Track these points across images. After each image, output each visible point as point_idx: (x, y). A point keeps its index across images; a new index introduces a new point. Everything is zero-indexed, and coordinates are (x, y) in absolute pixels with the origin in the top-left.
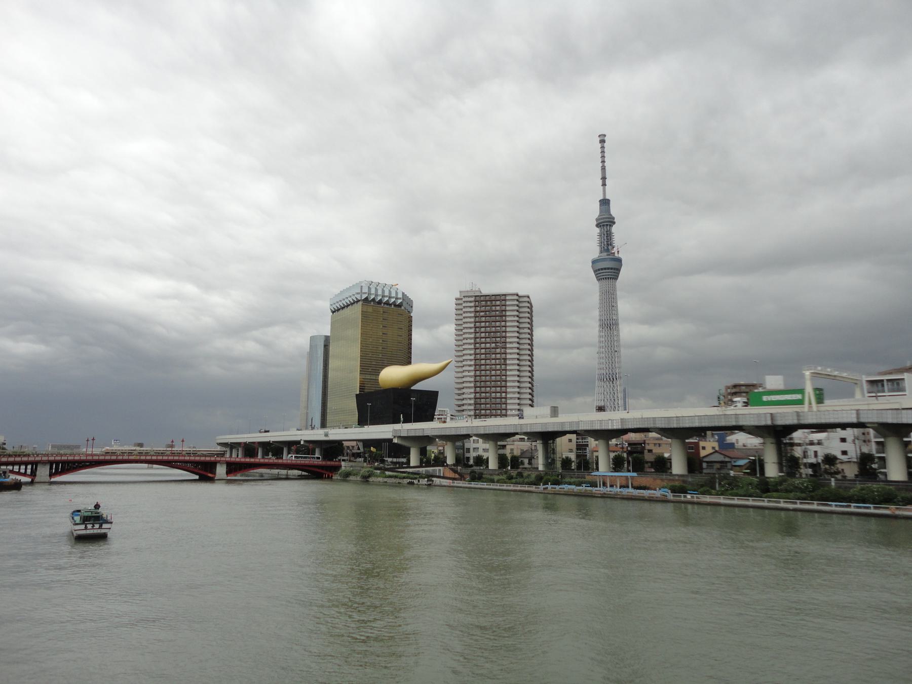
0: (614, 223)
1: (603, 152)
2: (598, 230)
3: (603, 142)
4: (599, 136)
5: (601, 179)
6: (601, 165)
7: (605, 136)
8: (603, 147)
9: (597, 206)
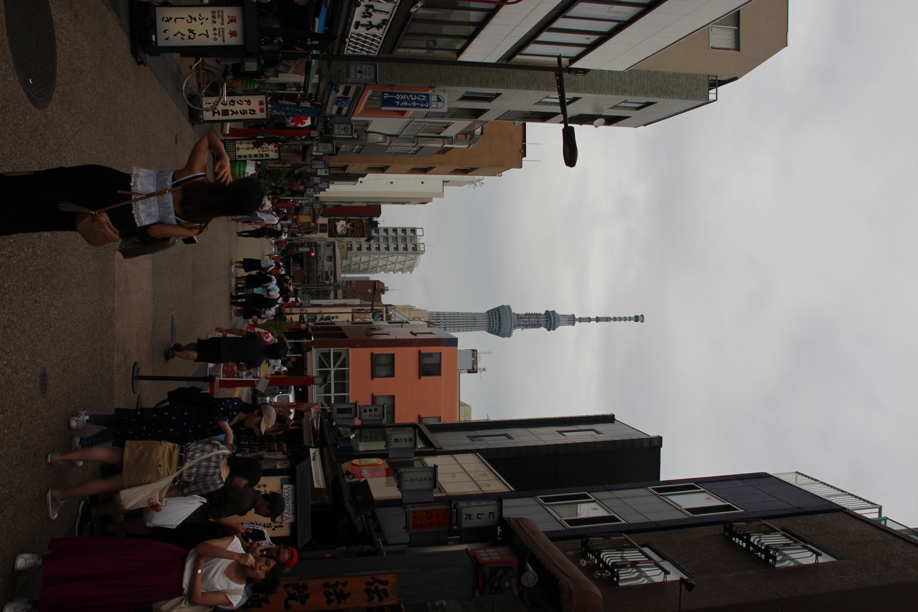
0: (549, 330)
2: (543, 312)
3: (637, 319)
4: (642, 315)
6: (612, 317)
7: (642, 322)
8: (630, 319)
9: (569, 312)
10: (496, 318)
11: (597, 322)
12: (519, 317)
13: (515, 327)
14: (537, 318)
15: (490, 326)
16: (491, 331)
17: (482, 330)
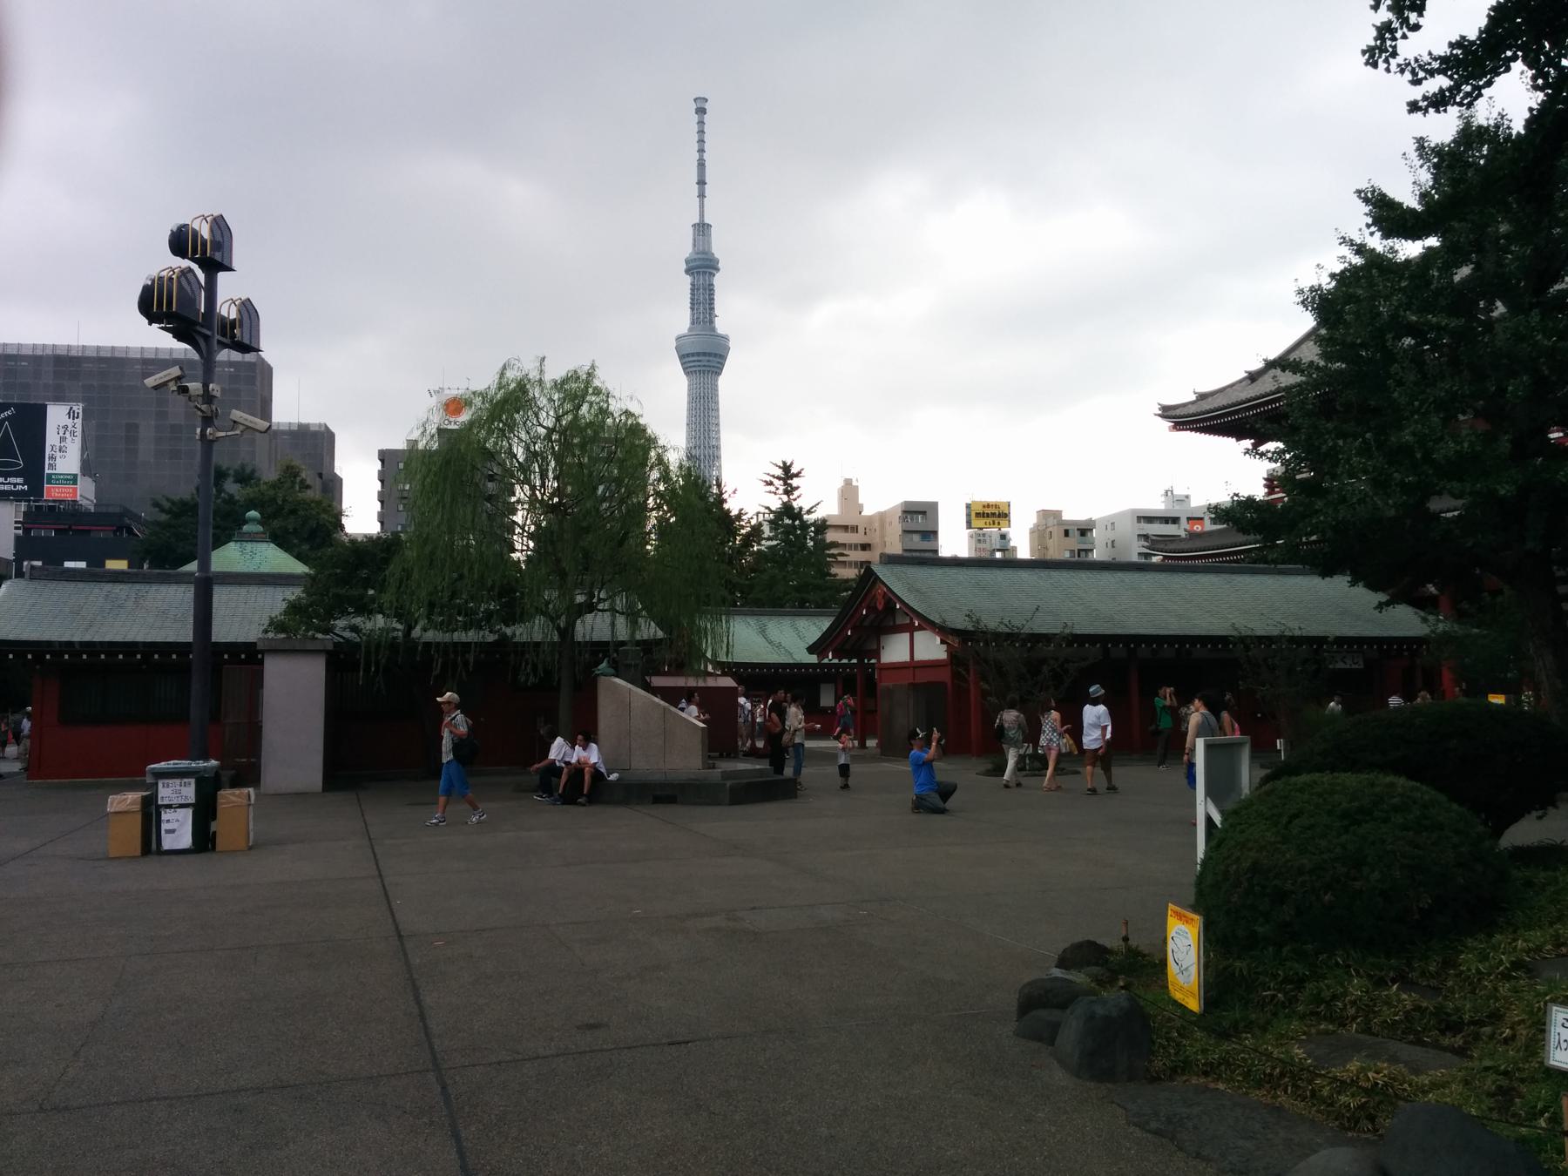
1: (701, 132)
3: (701, 111)
4: (695, 100)
5: (698, 183)
6: (697, 156)
7: (706, 100)
8: (701, 123)
11: (706, 183)
13: (714, 329)
14: (698, 289)
15: (709, 371)
16: (718, 371)
17: (717, 386)
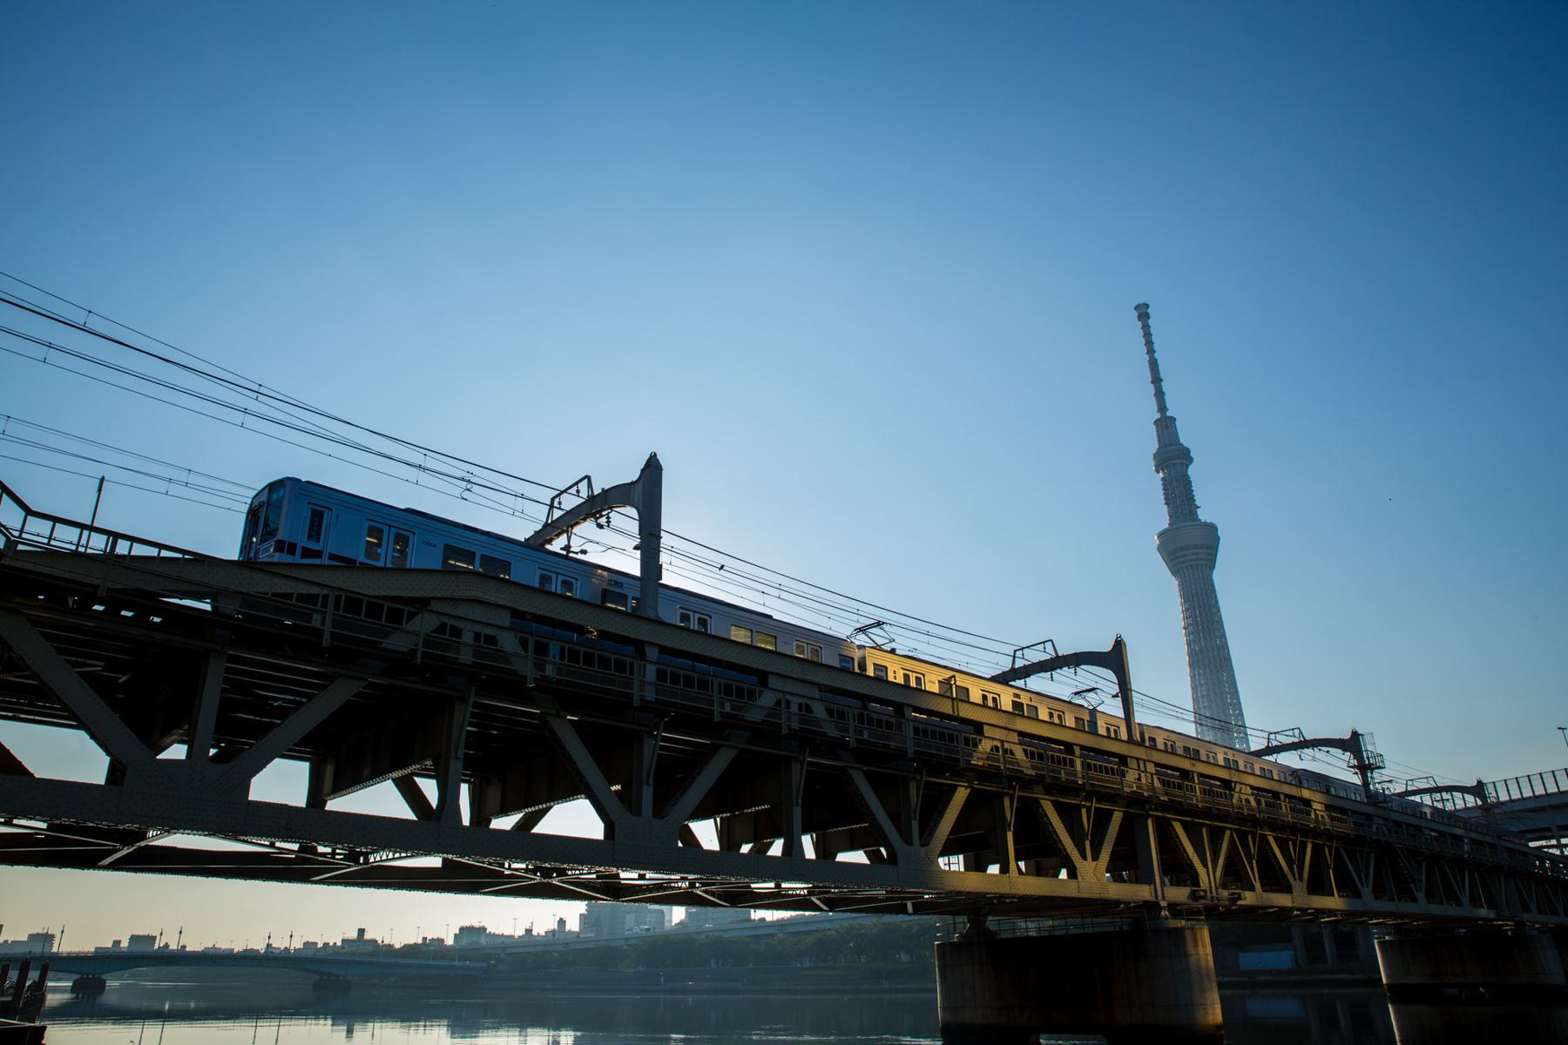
1: (1147, 334)
4: (1136, 308)
6: (1147, 357)
7: (1147, 306)
9: (1152, 431)
10: (1185, 555)
12: (1173, 516)
